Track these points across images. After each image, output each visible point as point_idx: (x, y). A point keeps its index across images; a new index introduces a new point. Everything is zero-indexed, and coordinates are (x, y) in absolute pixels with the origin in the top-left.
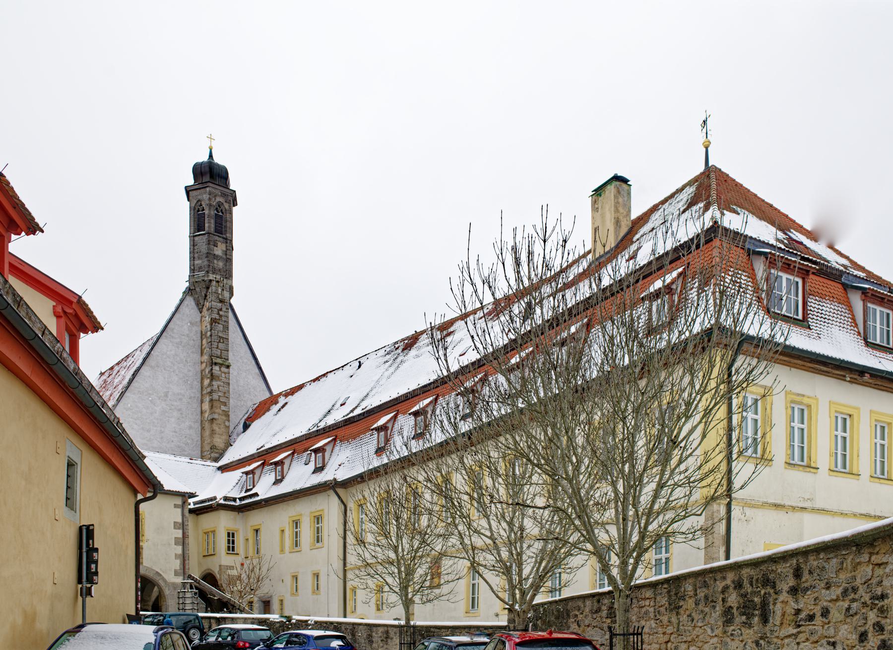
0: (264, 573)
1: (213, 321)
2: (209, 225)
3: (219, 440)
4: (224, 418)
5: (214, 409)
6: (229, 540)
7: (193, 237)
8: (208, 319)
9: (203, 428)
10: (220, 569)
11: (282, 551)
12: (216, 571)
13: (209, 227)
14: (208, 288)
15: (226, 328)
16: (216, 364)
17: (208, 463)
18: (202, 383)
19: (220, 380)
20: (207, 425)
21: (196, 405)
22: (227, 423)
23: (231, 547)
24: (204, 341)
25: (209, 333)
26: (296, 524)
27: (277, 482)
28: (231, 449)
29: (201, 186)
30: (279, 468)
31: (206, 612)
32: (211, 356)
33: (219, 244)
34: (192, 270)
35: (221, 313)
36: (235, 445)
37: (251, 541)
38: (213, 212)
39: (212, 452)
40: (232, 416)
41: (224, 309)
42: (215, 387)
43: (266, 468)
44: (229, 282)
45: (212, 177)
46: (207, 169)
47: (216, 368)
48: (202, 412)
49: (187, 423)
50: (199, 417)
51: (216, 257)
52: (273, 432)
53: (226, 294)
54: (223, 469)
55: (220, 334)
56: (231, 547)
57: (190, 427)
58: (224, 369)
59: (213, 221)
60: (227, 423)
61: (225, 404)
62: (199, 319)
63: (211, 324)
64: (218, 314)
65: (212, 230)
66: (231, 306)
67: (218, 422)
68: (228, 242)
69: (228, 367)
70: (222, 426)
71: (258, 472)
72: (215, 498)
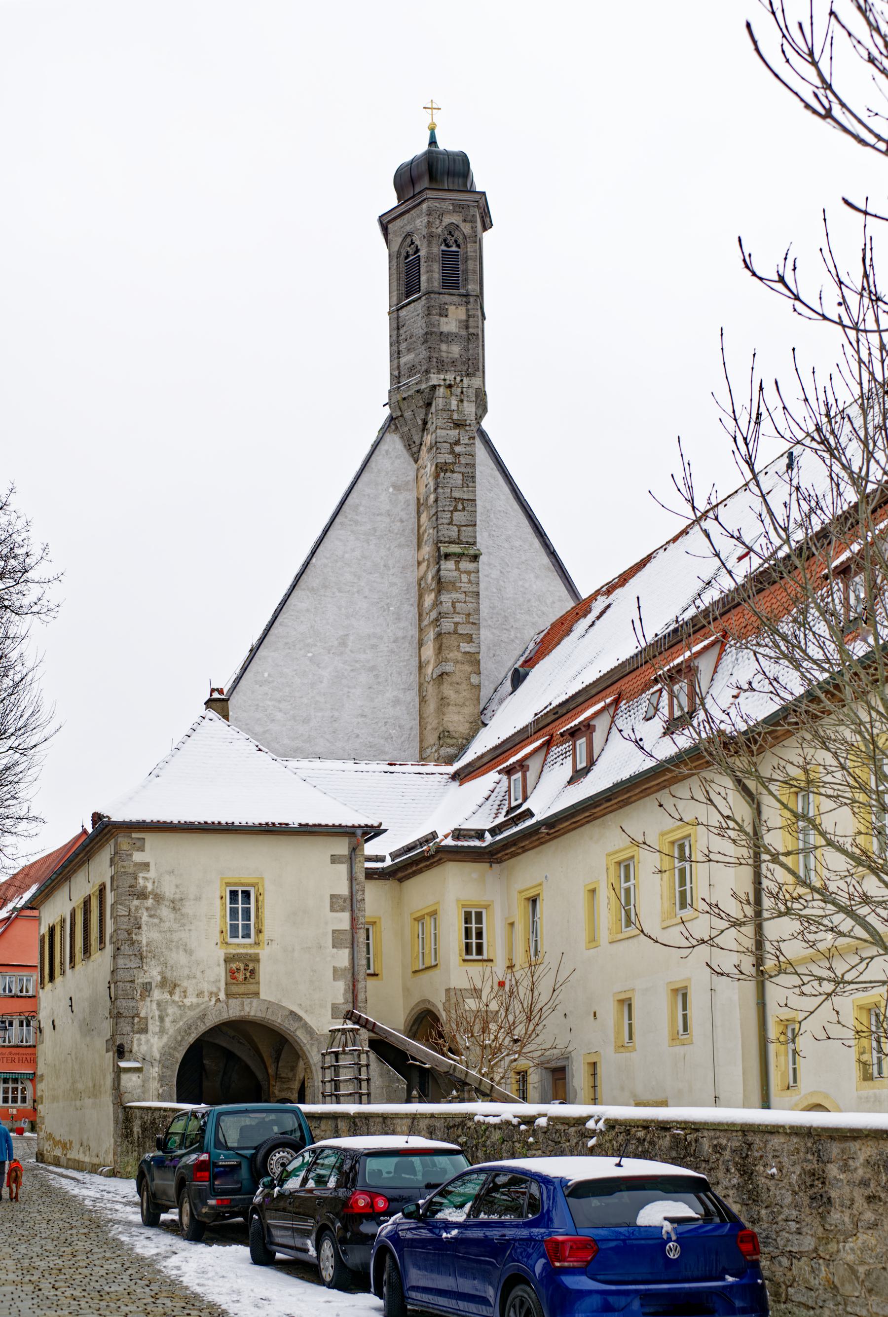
0: (544, 999)
1: (441, 469)
2: (430, 276)
3: (456, 718)
4: (467, 668)
5: (445, 653)
7: (396, 312)
8: (430, 469)
9: (423, 700)
10: (448, 999)
11: (593, 940)
12: (439, 1002)
13: (429, 280)
14: (429, 405)
15: (470, 478)
16: (447, 556)
17: (431, 768)
18: (420, 605)
19: (457, 589)
20: (431, 690)
21: (408, 654)
22: (474, 679)
23: (474, 945)
24: (424, 517)
25: (432, 498)
26: (626, 867)
27: (578, 775)
28: (484, 732)
29: (410, 204)
30: (582, 742)
31: (408, 1101)
32: (438, 542)
33: (452, 309)
34: (396, 378)
35: (457, 449)
36: (492, 724)
37: (520, 928)
38: (437, 249)
39: (442, 746)
40: (486, 664)
41: (465, 440)
42: (447, 607)
43: (555, 750)
44: (476, 382)
45: (432, 177)
46: (424, 167)
47: (450, 565)
48: (421, 667)
49: (390, 694)
50: (414, 678)
51: (445, 337)
52: (573, 672)
53: (470, 409)
54: (461, 777)
55: (456, 494)
56: (474, 945)
57: (396, 702)
58: (465, 565)
59: (436, 267)
60: (474, 679)
61: (469, 639)
62: (412, 475)
63: (437, 476)
64: (452, 452)
65: (436, 285)
66: (483, 435)
67: (455, 679)
68: (474, 301)
69: (475, 558)
70: (464, 686)
71: (534, 765)
72: (434, 835)
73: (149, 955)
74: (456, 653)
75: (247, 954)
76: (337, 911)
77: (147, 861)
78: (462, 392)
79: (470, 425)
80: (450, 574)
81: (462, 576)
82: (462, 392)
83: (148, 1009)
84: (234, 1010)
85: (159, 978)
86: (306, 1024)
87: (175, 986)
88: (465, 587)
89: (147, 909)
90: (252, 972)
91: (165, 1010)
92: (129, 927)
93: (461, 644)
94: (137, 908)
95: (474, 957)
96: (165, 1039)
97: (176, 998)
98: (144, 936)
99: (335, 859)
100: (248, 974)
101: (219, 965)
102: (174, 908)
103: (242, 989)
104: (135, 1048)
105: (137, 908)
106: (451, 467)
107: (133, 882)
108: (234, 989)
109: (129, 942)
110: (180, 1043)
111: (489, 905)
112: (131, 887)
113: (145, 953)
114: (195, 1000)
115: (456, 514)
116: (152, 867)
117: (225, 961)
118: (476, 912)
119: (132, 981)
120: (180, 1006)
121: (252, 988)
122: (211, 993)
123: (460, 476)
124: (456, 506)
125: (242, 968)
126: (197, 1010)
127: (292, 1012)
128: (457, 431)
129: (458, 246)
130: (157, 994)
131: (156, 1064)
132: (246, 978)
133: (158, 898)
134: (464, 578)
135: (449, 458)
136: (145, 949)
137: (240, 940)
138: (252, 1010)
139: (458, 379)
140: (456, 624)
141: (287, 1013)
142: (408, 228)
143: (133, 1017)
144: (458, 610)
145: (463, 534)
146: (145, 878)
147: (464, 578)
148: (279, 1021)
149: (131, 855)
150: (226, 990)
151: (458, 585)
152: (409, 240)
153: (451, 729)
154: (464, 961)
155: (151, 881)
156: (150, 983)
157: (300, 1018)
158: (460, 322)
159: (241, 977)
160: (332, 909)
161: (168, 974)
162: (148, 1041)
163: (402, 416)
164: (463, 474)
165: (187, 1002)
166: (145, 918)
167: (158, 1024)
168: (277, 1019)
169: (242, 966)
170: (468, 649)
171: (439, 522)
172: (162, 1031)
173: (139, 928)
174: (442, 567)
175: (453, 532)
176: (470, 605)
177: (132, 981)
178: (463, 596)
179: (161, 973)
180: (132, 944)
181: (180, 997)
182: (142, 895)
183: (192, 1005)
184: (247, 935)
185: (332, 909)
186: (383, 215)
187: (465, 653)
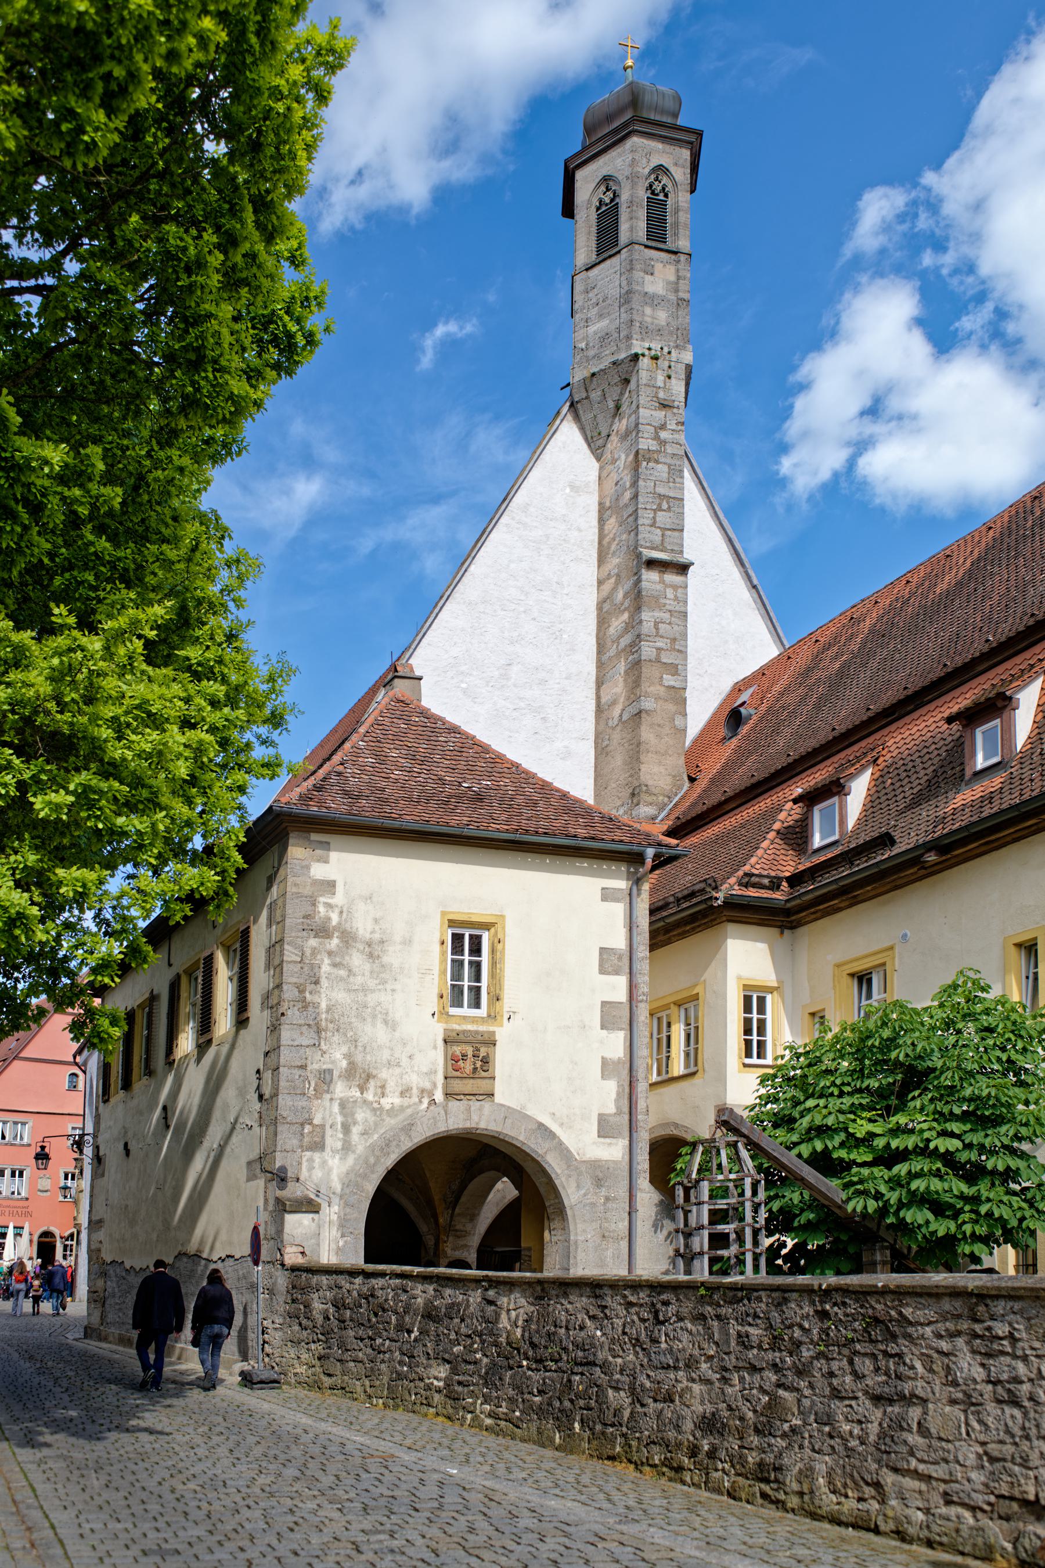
3: (656, 769)
4: (671, 707)
19: (661, 607)
35: (663, 435)
41: (672, 425)
42: (647, 627)
55: (660, 490)
58: (671, 578)
64: (657, 437)
70: (667, 730)
73: (331, 1026)
74: (658, 687)
76: (609, 974)
77: (332, 878)
80: (654, 587)
83: (326, 1112)
84: (457, 1118)
85: (344, 1064)
86: (561, 1143)
87: (369, 1076)
88: (671, 604)
89: (330, 953)
91: (353, 1114)
92: (302, 981)
94: (314, 952)
95: (754, 1060)
96: (351, 1160)
97: (370, 1096)
98: (323, 995)
99: (607, 895)
101: (435, 1047)
102: (371, 955)
103: (469, 1086)
104: (304, 1174)
105: (314, 952)
107: (309, 909)
108: (458, 1086)
109: (300, 1005)
110: (372, 1168)
112: (306, 917)
113: (323, 1024)
114: (397, 1101)
115: (659, 513)
116: (340, 888)
117: (445, 1041)
119: (303, 1067)
120: (374, 1110)
121: (482, 1085)
122: (423, 1091)
123: (665, 468)
124: (660, 505)
125: (470, 1053)
126: (401, 1117)
127: (541, 1126)
130: (340, 1089)
131: (336, 1200)
132: (475, 1069)
133: (348, 938)
135: (653, 445)
136: (324, 1016)
137: (466, 1011)
138: (481, 1119)
141: (535, 1126)
143: (302, 1125)
144: (661, 632)
145: (667, 540)
146: (329, 906)
148: (521, 1138)
149: (308, 867)
150: (446, 1086)
151: (662, 601)
153: (650, 783)
154: (745, 1065)
155: (337, 911)
156: (330, 1071)
157: (552, 1135)
158: (669, 283)
159: (468, 1067)
160: (602, 971)
161: (359, 1058)
162: (324, 1163)
164: (669, 466)
165: (386, 1102)
166: (326, 968)
167: (341, 1136)
168: (520, 1135)
169: (469, 1051)
171: (640, 522)
172: (347, 1147)
174: (644, 577)
176: (676, 628)
177: (303, 1067)
179: (348, 1056)
181: (375, 1094)
182: (323, 931)
183: (392, 1108)
184: (477, 1005)
185: (602, 971)
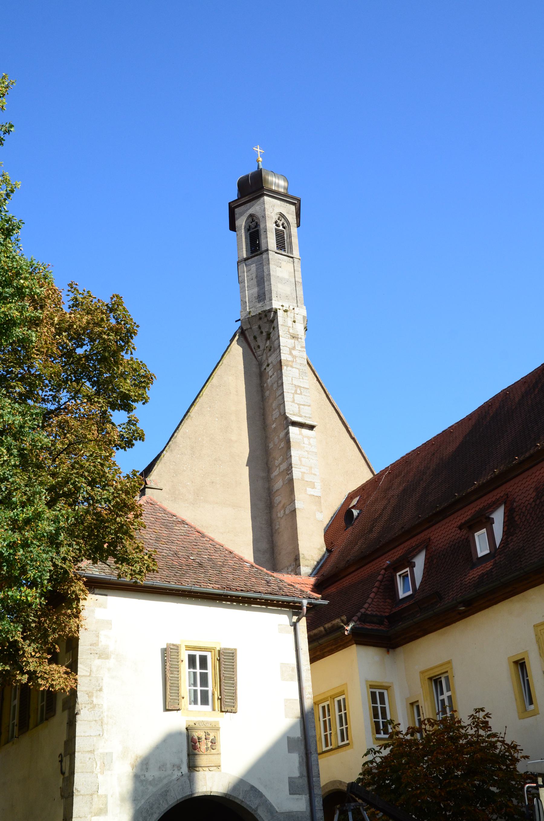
6: (375, 709)
33: (283, 264)
35: (294, 352)
41: (298, 347)
55: (296, 382)
64: (291, 354)
75: (207, 722)
78: (294, 317)
79: (301, 338)
81: (305, 439)
82: (294, 317)
90: (213, 742)
93: (307, 489)
100: (210, 744)
106: (290, 363)
109: (89, 706)
111: (390, 687)
115: (296, 396)
118: (379, 693)
119: (92, 752)
124: (296, 391)
125: (204, 737)
128: (293, 341)
129: (284, 228)
134: (306, 441)
135: (290, 358)
137: (200, 707)
139: (291, 308)
140: (303, 473)
142: (251, 211)
147: (306, 441)
152: (250, 219)
156: (111, 754)
163: (251, 328)
170: (312, 493)
173: (101, 690)
175: (295, 408)
178: (306, 453)
180: (94, 706)
182: (104, 655)
183: (154, 780)
186: (232, 202)
187: (311, 495)
